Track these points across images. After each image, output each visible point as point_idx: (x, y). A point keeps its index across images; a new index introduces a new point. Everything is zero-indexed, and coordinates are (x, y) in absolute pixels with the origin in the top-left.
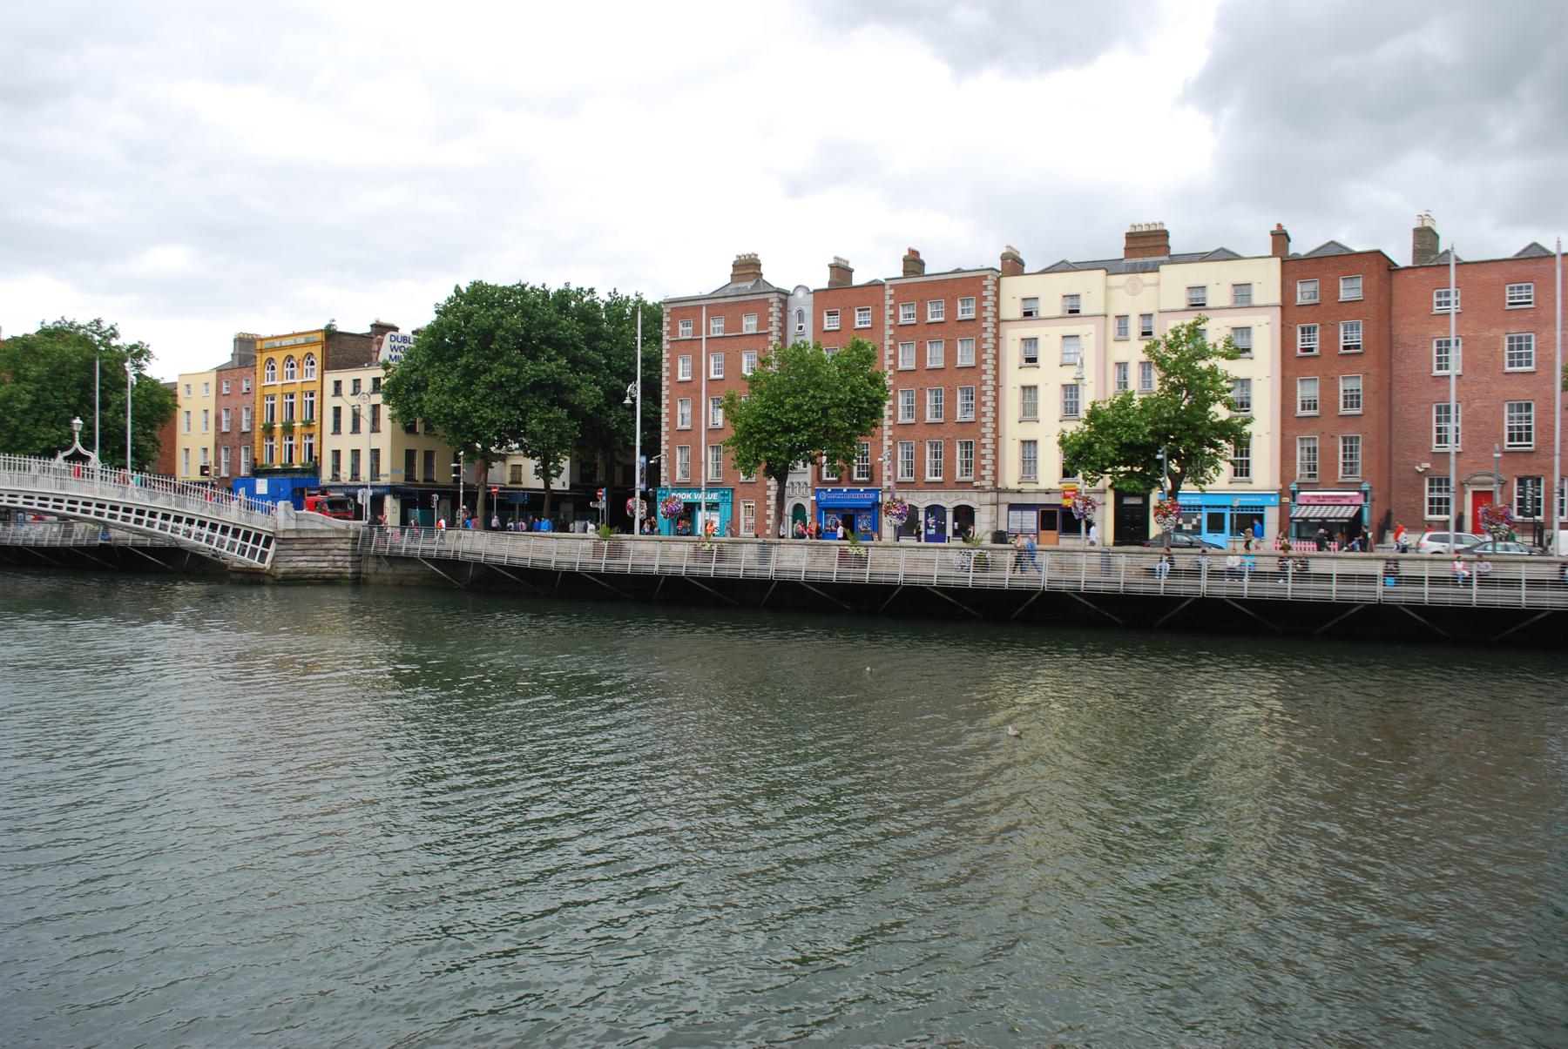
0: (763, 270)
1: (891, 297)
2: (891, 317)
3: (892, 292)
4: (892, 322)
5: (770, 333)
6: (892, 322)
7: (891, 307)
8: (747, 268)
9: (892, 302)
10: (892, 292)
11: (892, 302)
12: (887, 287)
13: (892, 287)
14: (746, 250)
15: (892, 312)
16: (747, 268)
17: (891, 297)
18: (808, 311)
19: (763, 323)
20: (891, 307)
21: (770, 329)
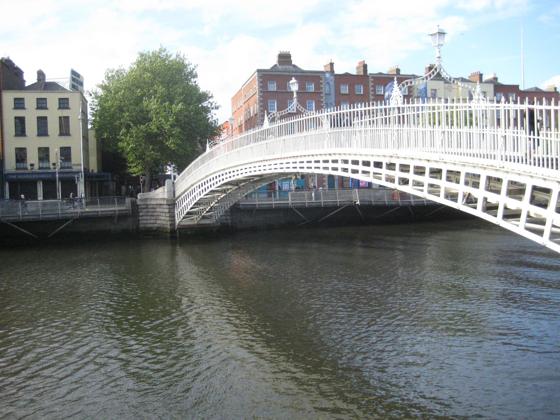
0: (292, 59)
1: (372, 82)
2: (373, 91)
3: (372, 80)
4: (373, 93)
5: (322, 93)
6: (373, 93)
7: (372, 86)
8: (285, 58)
9: (372, 84)
10: (372, 80)
11: (372, 84)
12: (370, 77)
13: (372, 77)
14: (285, 50)
15: (372, 89)
16: (285, 58)
17: (372, 82)
18: (332, 83)
19: (318, 87)
20: (372, 86)
21: (321, 91)
